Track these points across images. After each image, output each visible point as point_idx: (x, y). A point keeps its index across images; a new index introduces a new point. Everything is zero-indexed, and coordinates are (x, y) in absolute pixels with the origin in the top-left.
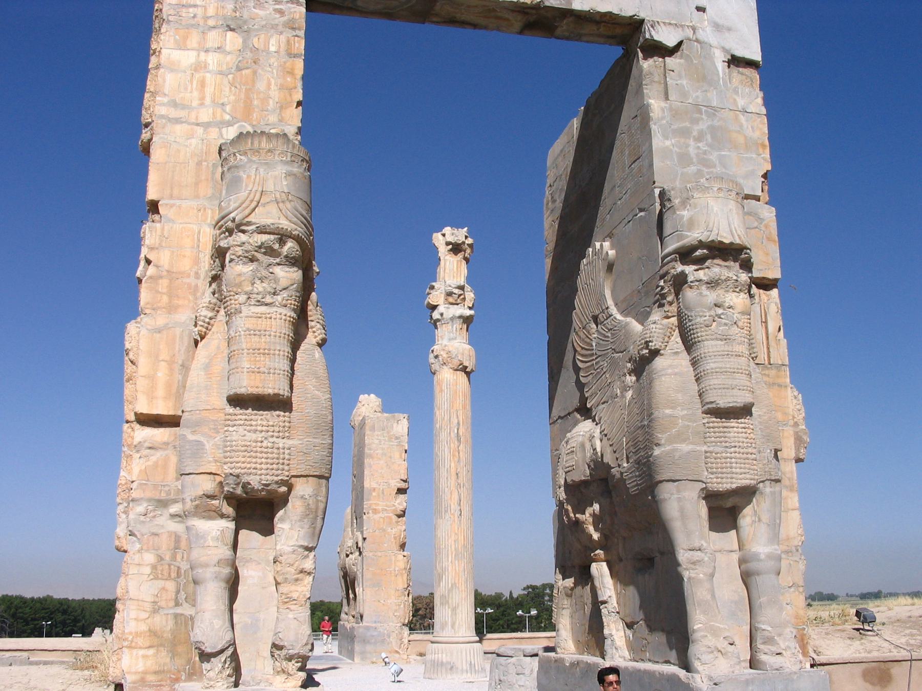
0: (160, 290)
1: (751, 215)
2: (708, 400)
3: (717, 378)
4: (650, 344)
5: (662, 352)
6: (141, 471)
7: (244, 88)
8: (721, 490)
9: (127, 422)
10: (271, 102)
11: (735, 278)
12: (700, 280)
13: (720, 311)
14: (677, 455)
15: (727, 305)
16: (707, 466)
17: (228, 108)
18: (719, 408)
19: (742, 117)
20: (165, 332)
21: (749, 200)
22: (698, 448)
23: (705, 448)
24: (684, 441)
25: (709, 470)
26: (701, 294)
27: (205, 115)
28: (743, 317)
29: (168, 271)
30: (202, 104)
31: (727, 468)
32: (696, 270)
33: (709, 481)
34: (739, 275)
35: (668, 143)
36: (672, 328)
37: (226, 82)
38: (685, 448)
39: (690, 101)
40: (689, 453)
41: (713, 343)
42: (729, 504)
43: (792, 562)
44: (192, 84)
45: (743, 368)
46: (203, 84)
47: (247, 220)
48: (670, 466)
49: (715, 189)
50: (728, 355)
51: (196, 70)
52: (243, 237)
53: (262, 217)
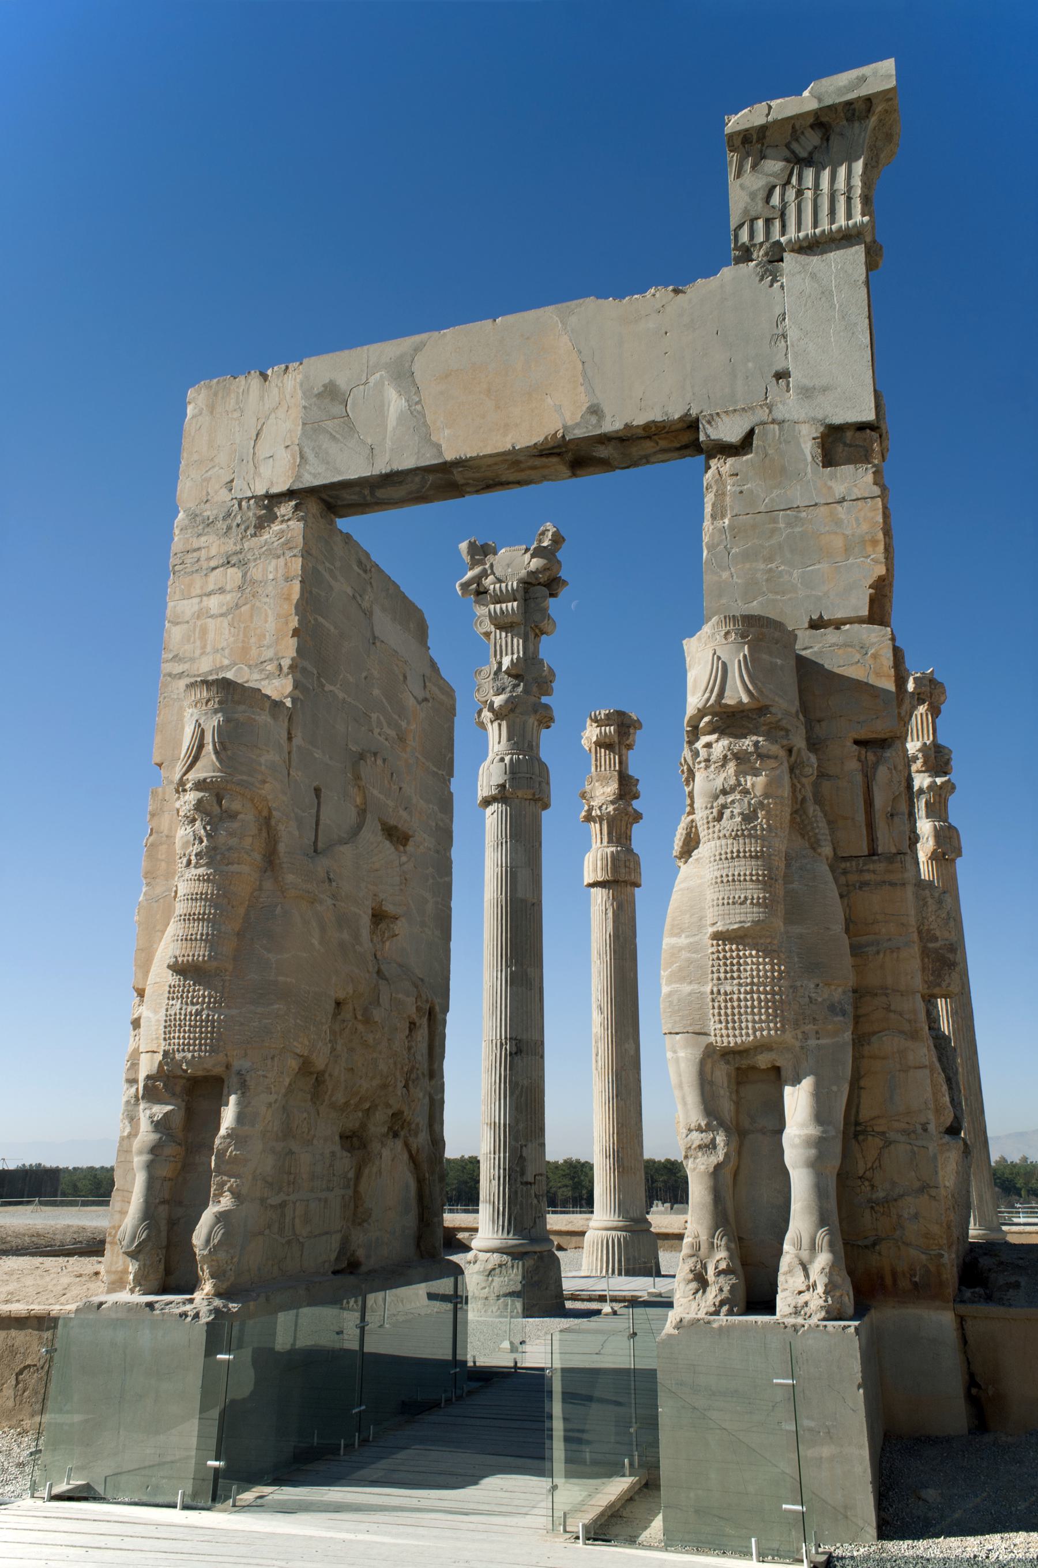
0: (159, 857)
1: (851, 646)
2: (708, 923)
7: (242, 626)
10: (267, 637)
17: (227, 651)
18: (722, 933)
19: (840, 509)
20: (161, 900)
21: (848, 626)
22: (702, 989)
24: (682, 980)
28: (766, 802)
29: (167, 836)
30: (202, 654)
35: (725, 575)
37: (226, 624)
38: (686, 988)
39: (762, 509)
40: (690, 994)
42: (763, 1061)
43: (915, 1148)
44: (194, 634)
45: (760, 873)
46: (204, 631)
47: (185, 778)
49: (723, 633)
51: (198, 617)
53: (198, 773)
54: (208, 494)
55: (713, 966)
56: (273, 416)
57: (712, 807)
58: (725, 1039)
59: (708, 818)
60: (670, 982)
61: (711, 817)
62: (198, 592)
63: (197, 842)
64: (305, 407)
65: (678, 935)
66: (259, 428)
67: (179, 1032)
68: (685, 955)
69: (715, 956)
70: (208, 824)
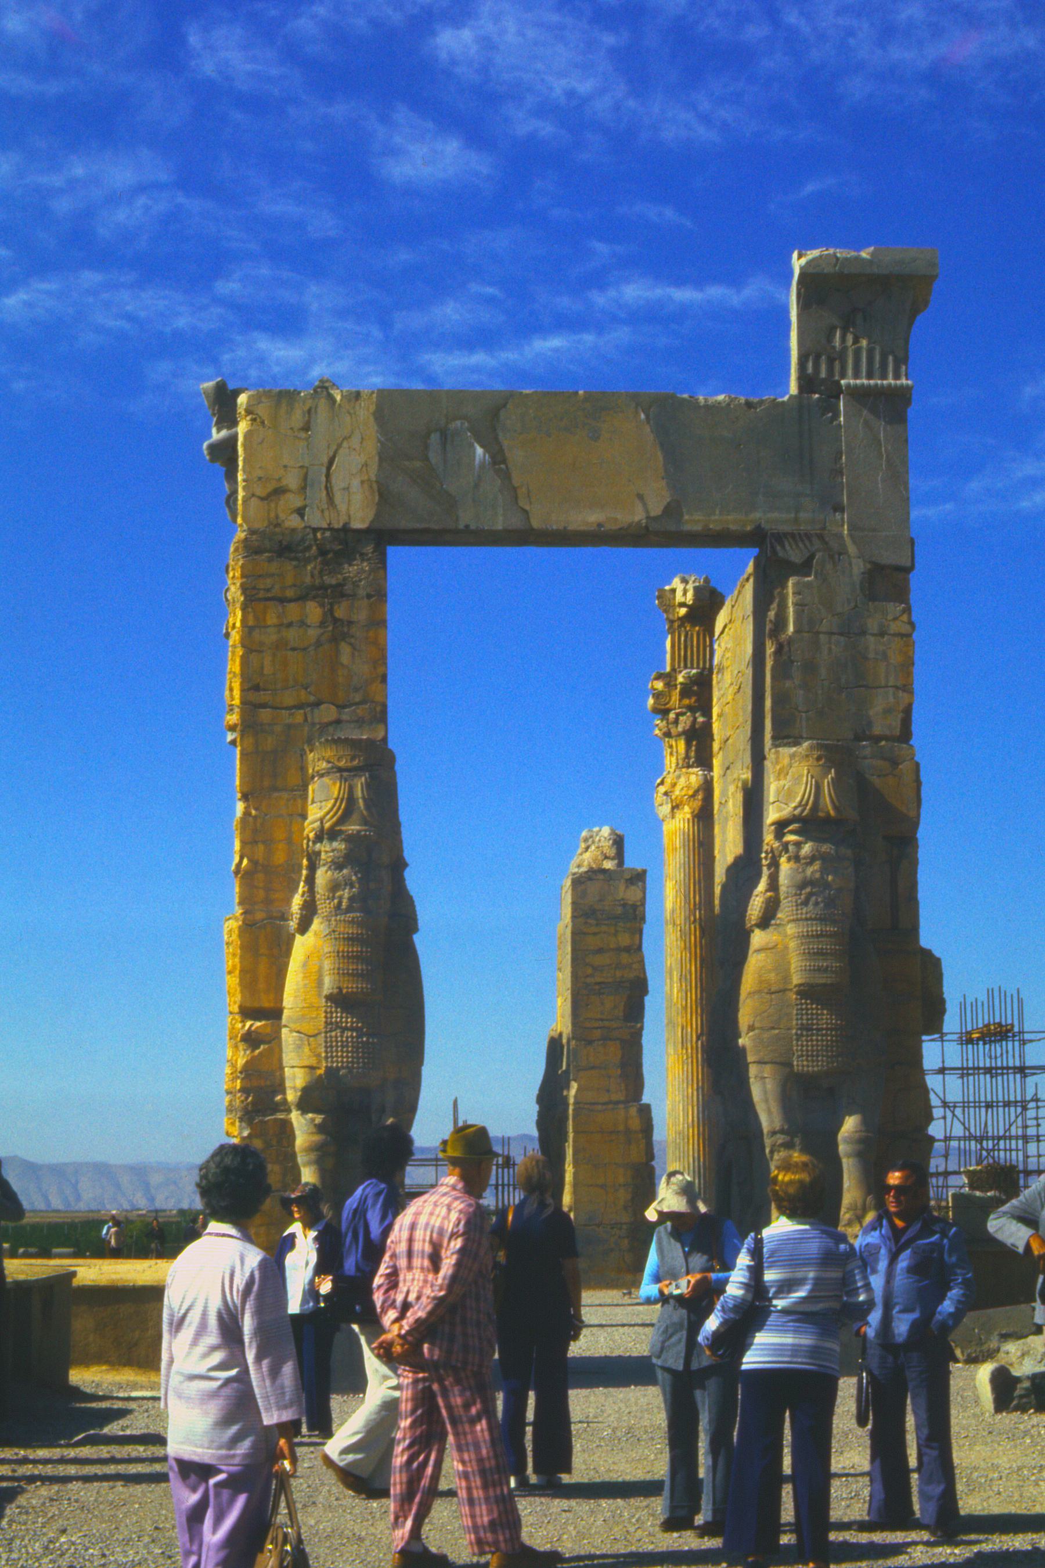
6: (247, 1062)
9: (231, 1013)
27: (289, 699)
52: (335, 844)
54: (277, 517)
55: (797, 1014)
56: (345, 444)
57: (800, 894)
58: (800, 1068)
59: (796, 902)
61: (799, 901)
62: (275, 621)
63: (348, 887)
64: (379, 441)
66: (331, 454)
67: (342, 1051)
69: (799, 1007)
70: (358, 872)
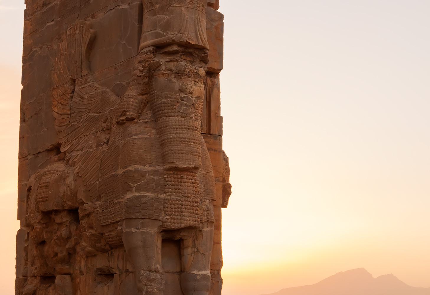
3: (177, 145)
4: (128, 113)
5: (136, 121)
8: (173, 227)
11: (196, 71)
12: (171, 70)
13: (183, 95)
14: (144, 200)
15: (188, 90)
16: (165, 209)
23: (162, 196)
25: (166, 212)
26: (170, 80)
31: (178, 211)
32: (168, 62)
33: (165, 220)
34: (199, 69)
36: (144, 103)
38: (151, 195)
41: (177, 118)
42: (178, 237)
48: (138, 208)
50: (186, 128)
60: (138, 189)
65: (144, 165)
68: (149, 177)
